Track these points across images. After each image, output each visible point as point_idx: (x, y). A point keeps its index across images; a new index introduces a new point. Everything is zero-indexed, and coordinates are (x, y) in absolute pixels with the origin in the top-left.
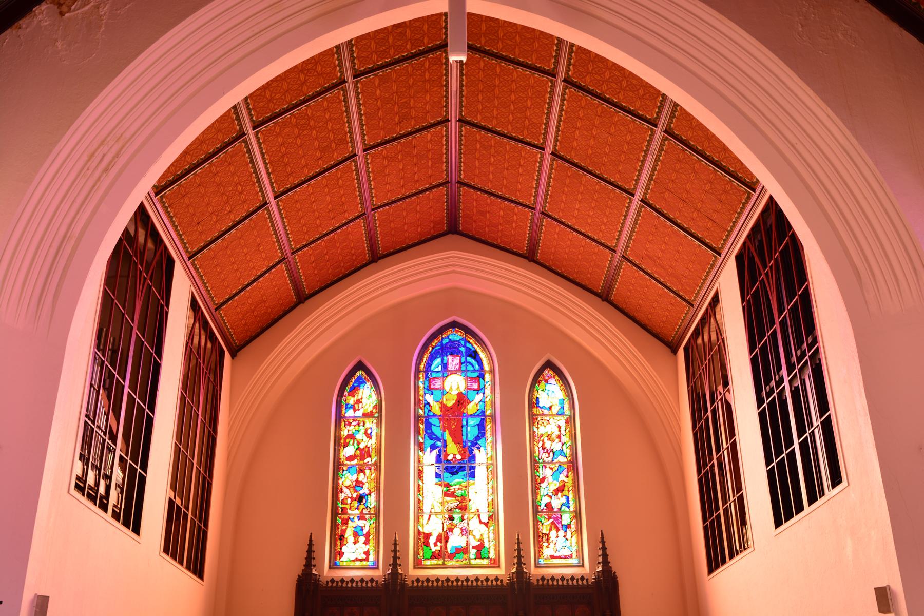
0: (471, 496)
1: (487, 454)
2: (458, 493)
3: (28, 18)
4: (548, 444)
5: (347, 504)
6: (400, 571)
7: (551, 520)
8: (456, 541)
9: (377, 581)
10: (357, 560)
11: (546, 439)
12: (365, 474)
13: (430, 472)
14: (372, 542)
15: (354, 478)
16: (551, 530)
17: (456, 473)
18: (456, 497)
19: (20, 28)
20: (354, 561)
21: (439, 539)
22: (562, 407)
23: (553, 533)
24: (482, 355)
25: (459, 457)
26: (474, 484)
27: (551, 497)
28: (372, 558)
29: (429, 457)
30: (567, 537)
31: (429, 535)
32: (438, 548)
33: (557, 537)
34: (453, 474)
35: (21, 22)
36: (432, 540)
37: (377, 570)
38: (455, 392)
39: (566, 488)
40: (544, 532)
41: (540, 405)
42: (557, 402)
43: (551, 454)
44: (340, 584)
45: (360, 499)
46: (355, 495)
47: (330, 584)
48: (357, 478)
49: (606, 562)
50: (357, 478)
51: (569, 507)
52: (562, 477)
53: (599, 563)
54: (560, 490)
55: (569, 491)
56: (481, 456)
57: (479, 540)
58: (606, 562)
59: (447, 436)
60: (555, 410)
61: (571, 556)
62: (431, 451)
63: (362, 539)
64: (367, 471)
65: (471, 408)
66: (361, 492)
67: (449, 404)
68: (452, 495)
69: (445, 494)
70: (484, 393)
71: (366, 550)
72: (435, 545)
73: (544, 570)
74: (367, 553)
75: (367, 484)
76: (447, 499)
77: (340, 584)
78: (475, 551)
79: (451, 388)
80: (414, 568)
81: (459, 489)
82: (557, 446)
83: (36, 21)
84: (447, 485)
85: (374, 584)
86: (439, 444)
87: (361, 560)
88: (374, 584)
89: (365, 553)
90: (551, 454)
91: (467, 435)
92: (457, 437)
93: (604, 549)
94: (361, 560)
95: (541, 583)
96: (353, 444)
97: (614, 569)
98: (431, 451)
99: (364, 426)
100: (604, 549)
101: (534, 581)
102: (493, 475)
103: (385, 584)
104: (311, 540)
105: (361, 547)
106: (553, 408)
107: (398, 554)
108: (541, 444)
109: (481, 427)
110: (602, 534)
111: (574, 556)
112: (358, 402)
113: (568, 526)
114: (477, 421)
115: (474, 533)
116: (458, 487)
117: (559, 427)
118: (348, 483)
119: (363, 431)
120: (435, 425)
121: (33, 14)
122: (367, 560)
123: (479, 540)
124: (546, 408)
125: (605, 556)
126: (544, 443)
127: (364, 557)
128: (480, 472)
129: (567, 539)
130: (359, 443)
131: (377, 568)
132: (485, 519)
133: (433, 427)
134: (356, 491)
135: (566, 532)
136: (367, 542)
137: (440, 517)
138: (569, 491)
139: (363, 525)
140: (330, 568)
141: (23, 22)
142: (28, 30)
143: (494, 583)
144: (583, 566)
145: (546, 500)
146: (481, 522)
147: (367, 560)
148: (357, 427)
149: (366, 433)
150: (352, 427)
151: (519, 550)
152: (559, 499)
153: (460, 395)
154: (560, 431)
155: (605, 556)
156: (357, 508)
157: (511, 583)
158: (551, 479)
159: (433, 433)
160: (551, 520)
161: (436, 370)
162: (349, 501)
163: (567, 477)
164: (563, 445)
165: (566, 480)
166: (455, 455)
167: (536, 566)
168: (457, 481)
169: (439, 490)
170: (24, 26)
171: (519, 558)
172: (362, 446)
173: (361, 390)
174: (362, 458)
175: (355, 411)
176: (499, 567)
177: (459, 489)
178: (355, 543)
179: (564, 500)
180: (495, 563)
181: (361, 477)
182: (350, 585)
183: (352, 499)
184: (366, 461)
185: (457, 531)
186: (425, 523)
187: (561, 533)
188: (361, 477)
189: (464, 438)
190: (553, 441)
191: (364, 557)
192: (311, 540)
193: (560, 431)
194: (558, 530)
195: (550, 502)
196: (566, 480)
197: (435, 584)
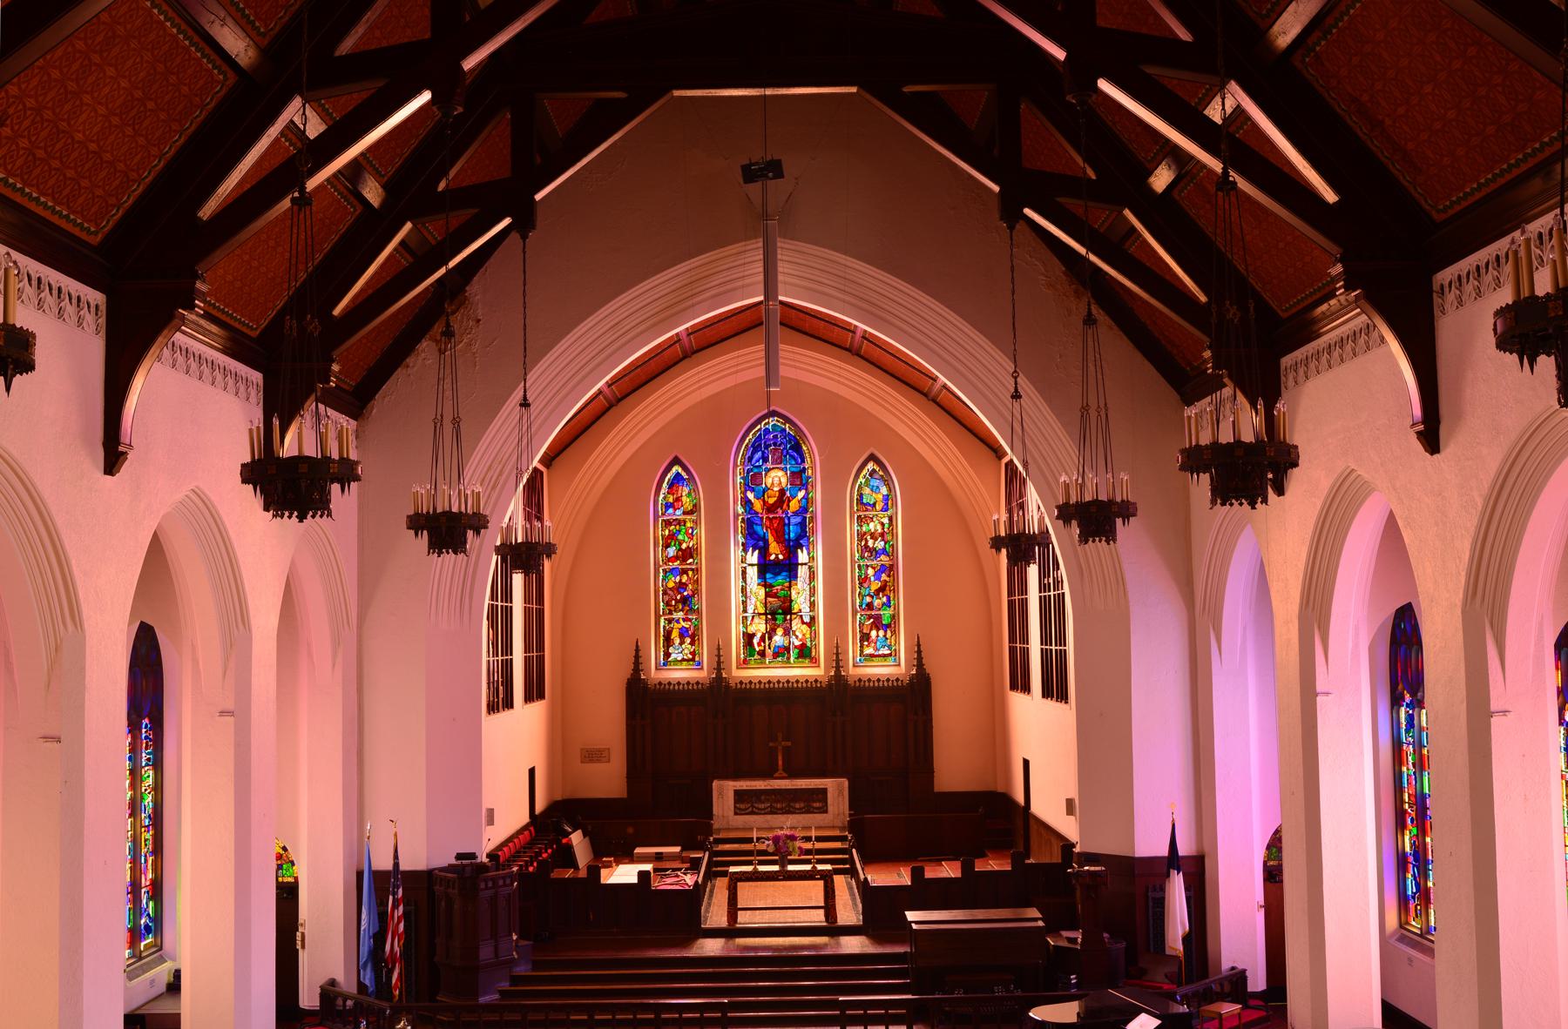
0: (794, 595)
1: (809, 554)
2: (782, 593)
3: (413, 356)
4: (870, 543)
5: (671, 606)
6: (724, 675)
7: (872, 620)
8: (779, 639)
9: (702, 684)
10: (683, 660)
11: (869, 537)
12: (688, 575)
13: (753, 573)
14: (697, 643)
15: (678, 578)
16: (871, 629)
17: (779, 574)
18: (778, 597)
19: (408, 367)
20: (681, 661)
21: (762, 639)
22: (887, 504)
23: (874, 633)
24: (804, 448)
25: (781, 557)
26: (796, 584)
27: (872, 597)
28: (697, 659)
29: (753, 557)
30: (888, 636)
31: (753, 635)
32: (762, 648)
33: (878, 636)
34: (776, 574)
35: (408, 360)
36: (756, 641)
37: (701, 671)
38: (776, 489)
39: (888, 588)
40: (864, 631)
41: (865, 501)
42: (881, 497)
43: (874, 553)
44: (667, 687)
45: (685, 600)
46: (678, 597)
47: (658, 686)
48: (681, 580)
49: (920, 665)
50: (681, 580)
51: (890, 607)
52: (884, 577)
53: (914, 666)
54: (882, 589)
55: (890, 591)
56: (803, 556)
57: (801, 640)
58: (920, 665)
59: (771, 539)
60: (878, 507)
61: (890, 655)
62: (753, 552)
63: (688, 640)
64: (690, 573)
65: (794, 505)
66: (685, 593)
67: (771, 501)
68: (775, 595)
69: (767, 595)
70: (806, 489)
71: (692, 650)
72: (759, 645)
73: (862, 669)
74: (693, 653)
75: (690, 587)
76: (770, 599)
77: (667, 687)
78: (797, 651)
79: (773, 484)
80: (737, 668)
81: (781, 590)
82: (880, 545)
83: (420, 358)
84: (771, 586)
85: (700, 686)
86: (761, 543)
87: (688, 660)
88: (700, 686)
89: (691, 653)
90: (874, 553)
91: (789, 534)
92: (780, 538)
93: (919, 652)
94: (688, 660)
95: (858, 684)
96: (675, 545)
97: (927, 671)
98: (753, 552)
99: (685, 525)
100: (919, 652)
101: (851, 682)
102: (812, 576)
103: (710, 687)
104: (637, 646)
105: (687, 646)
106: (877, 506)
107: (722, 658)
108: (863, 543)
109: (803, 524)
110: (918, 638)
111: (893, 654)
112: (678, 499)
113: (888, 626)
114: (798, 519)
115: (797, 633)
116: (779, 587)
117: (883, 524)
118: (671, 585)
119: (684, 531)
120: (757, 524)
121: (416, 352)
122: (693, 660)
123: (801, 640)
124: (870, 505)
125: (920, 659)
126: (867, 541)
127: (691, 657)
128: (802, 572)
129: (887, 639)
130: (680, 544)
131: (702, 668)
132: (807, 619)
133: (755, 526)
134: (680, 593)
135: (886, 632)
136: (692, 643)
137: (764, 617)
138: (890, 591)
139: (687, 626)
140: (656, 668)
141: (410, 360)
142: (415, 369)
143: (886, 684)
144: (899, 665)
145: (868, 599)
146: (803, 623)
147: (693, 660)
148: (678, 527)
149: (687, 533)
150: (673, 527)
151: (837, 654)
152: (880, 599)
153: (782, 492)
154: (883, 529)
155: (920, 659)
156: (682, 610)
157: (830, 685)
158: (872, 579)
159: (755, 533)
160: (872, 620)
161: (757, 464)
162: (673, 602)
163: (889, 576)
164: (885, 543)
165: (887, 579)
166: (777, 555)
167: (854, 666)
168: (779, 581)
169: (762, 592)
170: (411, 365)
171: (837, 658)
172: (684, 546)
173: (680, 488)
174: (684, 560)
175: (675, 510)
176: (819, 666)
177: (781, 590)
178: (681, 644)
179: (884, 599)
180: (815, 661)
181: (685, 579)
182: (676, 687)
183: (677, 601)
184: (689, 562)
185: (780, 631)
186: (749, 623)
187: (881, 633)
188: (685, 579)
189: (787, 537)
190: (876, 539)
191: (691, 657)
192: (637, 646)
193: (883, 529)
194: (878, 630)
195: (872, 602)
196: (887, 579)
197: (767, 686)
